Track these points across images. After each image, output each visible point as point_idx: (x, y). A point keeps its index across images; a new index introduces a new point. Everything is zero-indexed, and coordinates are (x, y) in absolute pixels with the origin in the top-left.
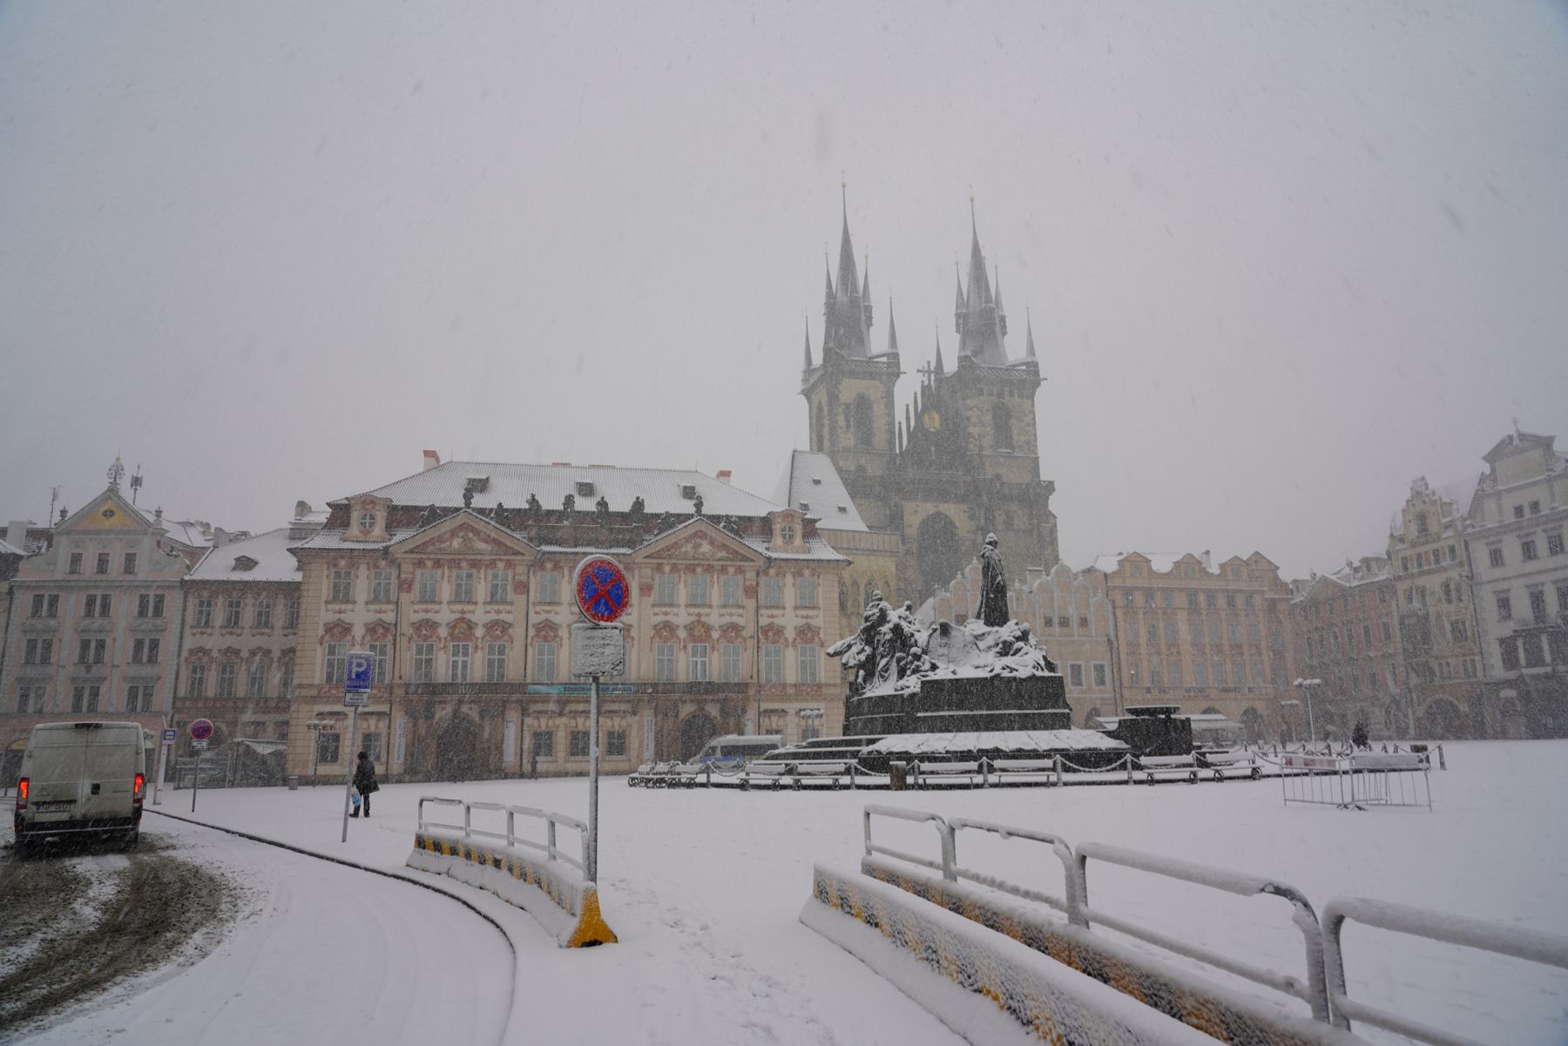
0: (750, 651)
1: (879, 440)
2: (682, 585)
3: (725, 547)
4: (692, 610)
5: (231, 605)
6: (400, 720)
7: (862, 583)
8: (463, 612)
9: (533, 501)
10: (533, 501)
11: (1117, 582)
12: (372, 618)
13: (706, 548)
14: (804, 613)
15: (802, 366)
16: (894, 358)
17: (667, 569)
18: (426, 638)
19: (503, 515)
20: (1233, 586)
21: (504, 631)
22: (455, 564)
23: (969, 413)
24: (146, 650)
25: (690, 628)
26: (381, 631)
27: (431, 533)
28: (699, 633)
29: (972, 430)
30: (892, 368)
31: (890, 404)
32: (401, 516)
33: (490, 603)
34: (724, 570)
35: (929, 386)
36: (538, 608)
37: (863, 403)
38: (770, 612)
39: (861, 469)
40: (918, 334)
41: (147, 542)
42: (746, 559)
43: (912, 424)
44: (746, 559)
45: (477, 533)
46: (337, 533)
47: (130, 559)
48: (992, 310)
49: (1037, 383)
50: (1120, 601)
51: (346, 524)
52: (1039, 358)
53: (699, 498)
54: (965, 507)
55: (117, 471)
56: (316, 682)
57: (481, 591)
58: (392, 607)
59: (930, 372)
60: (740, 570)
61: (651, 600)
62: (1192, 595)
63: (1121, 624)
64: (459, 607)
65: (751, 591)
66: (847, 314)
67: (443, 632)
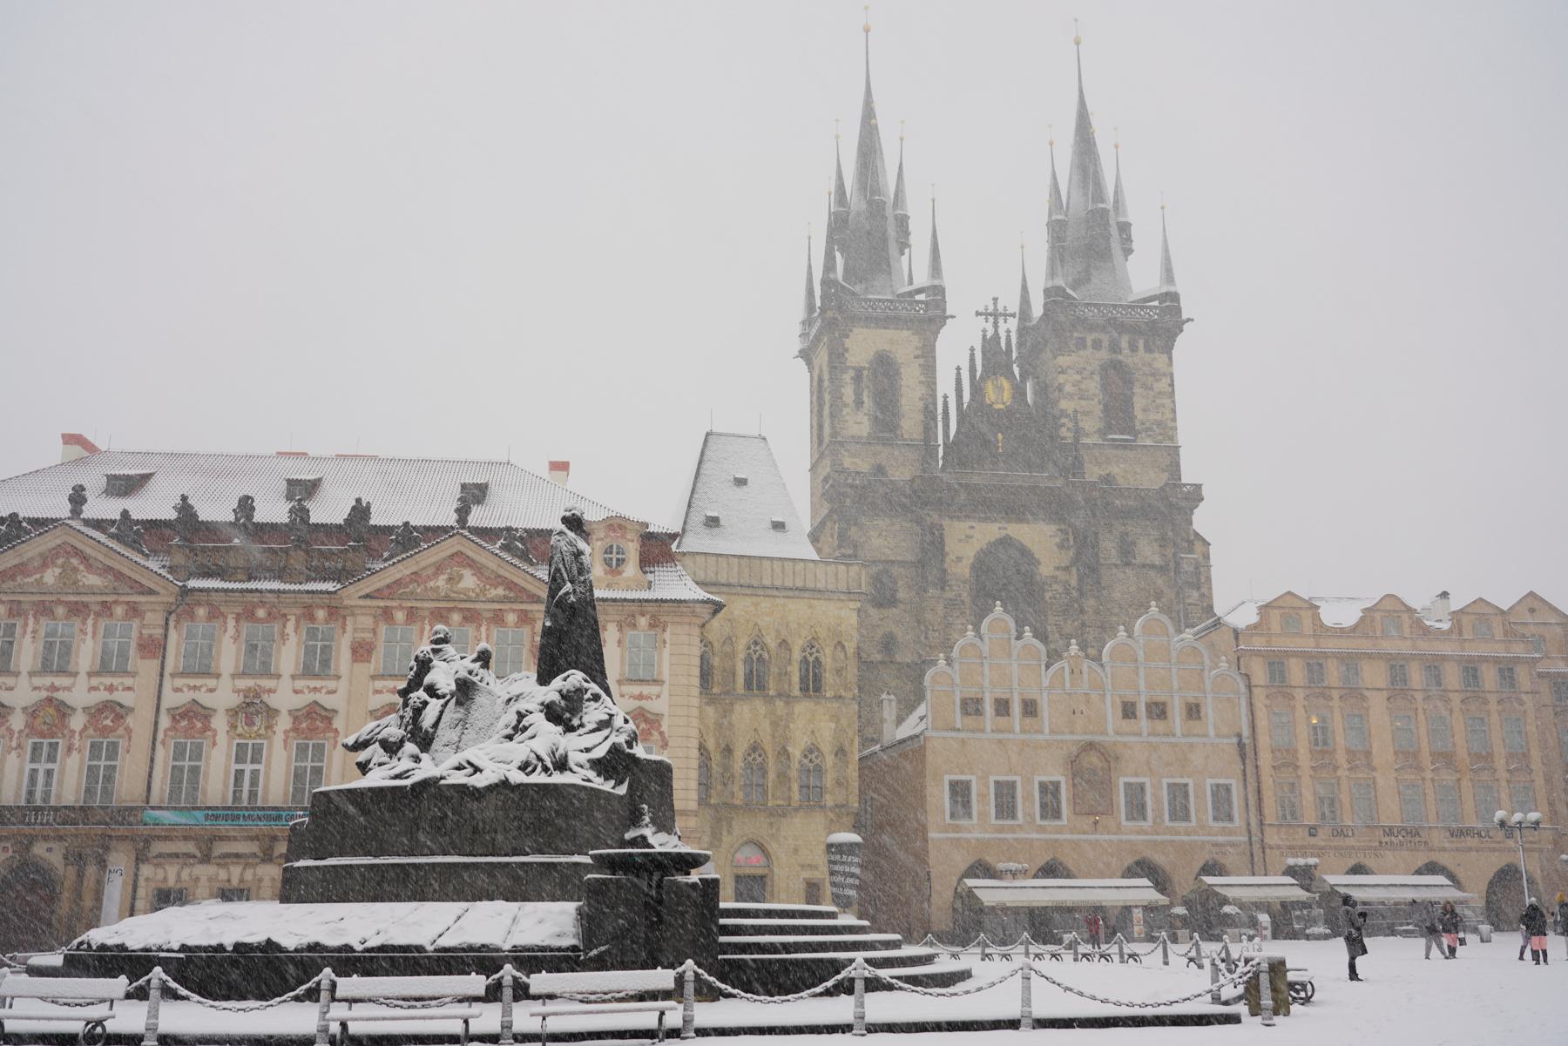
1: (910, 425)
8: (53, 688)
9: (185, 507)
10: (185, 507)
11: (1258, 643)
13: (469, 581)
15: (800, 313)
17: (400, 616)
19: (132, 532)
20: (1474, 651)
21: (119, 718)
22: (44, 610)
31: (929, 368)
35: (996, 335)
36: (179, 682)
37: (885, 366)
39: (880, 470)
43: (966, 397)
45: (85, 559)
48: (1105, 212)
49: (1179, 327)
50: (1260, 674)
52: (1179, 287)
57: (86, 654)
61: (371, 668)
62: (1397, 667)
64: (48, 680)
66: (866, 231)
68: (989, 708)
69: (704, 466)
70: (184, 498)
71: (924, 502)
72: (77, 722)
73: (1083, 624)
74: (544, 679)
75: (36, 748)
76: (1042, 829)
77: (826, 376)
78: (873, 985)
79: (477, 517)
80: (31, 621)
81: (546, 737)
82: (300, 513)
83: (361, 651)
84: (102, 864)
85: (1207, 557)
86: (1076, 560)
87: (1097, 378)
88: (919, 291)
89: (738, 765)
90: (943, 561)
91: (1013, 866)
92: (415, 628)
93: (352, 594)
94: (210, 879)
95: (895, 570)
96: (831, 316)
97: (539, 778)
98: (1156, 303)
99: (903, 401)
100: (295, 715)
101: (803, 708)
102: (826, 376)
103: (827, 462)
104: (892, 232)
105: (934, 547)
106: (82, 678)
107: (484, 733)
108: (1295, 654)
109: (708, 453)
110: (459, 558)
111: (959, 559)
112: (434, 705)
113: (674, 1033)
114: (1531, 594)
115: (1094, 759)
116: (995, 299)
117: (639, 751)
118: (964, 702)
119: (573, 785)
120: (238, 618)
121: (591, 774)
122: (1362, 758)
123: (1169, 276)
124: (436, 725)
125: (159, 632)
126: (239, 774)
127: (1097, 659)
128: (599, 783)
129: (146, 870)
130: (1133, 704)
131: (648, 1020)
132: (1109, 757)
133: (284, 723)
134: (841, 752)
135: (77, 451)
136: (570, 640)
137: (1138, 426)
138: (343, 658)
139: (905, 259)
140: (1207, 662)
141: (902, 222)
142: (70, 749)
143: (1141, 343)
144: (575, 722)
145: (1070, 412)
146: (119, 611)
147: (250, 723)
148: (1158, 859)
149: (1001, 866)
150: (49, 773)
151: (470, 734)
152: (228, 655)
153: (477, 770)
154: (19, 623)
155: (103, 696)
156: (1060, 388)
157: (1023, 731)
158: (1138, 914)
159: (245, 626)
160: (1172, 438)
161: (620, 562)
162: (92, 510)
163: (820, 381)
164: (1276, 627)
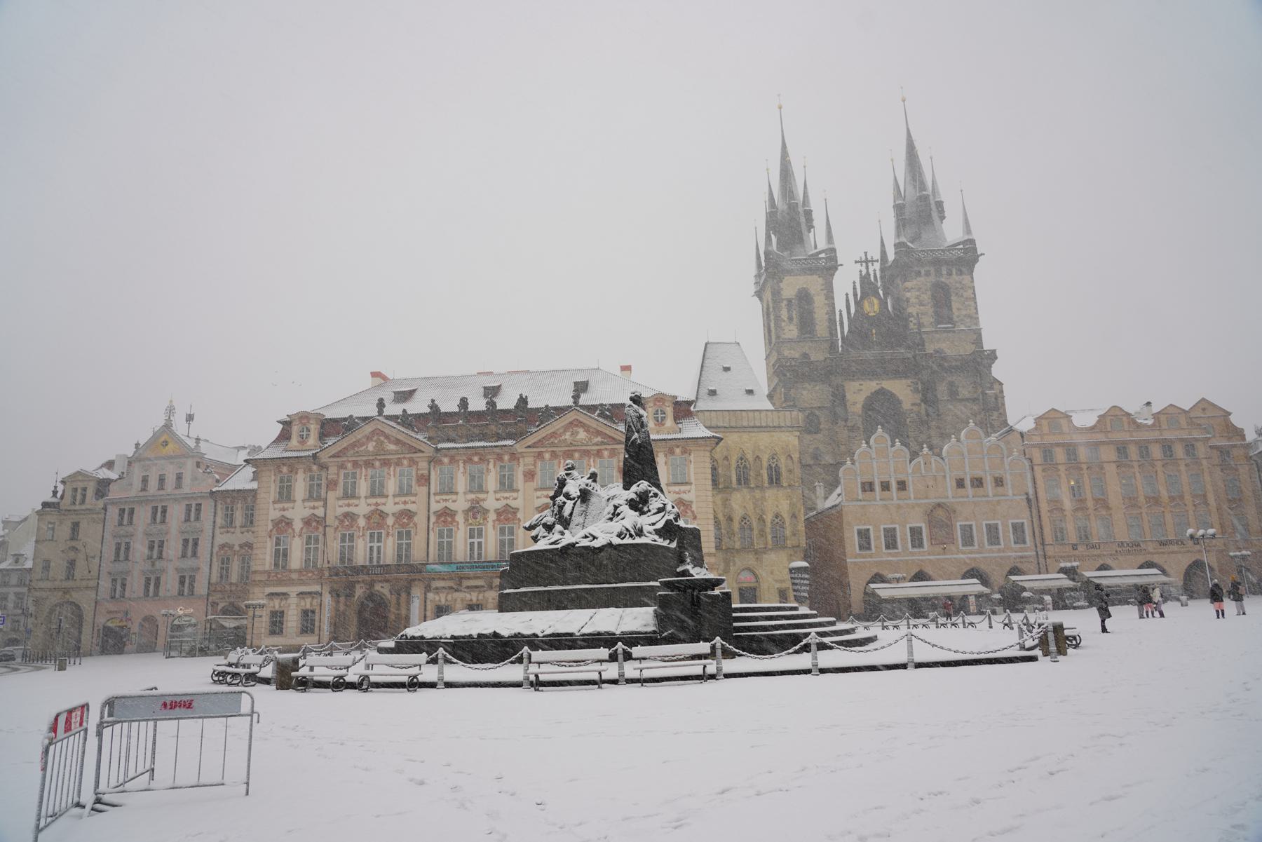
1: (821, 329)
3: (598, 433)
5: (247, 509)
6: (327, 599)
8: (377, 504)
9: (434, 406)
10: (434, 406)
11: (1037, 440)
12: (307, 513)
13: (582, 435)
14: (677, 488)
15: (753, 270)
17: (547, 456)
19: (406, 420)
20: (1169, 435)
22: (368, 464)
23: (908, 295)
24: (190, 546)
26: (314, 524)
27: (351, 439)
32: (330, 427)
33: (399, 495)
34: (599, 453)
36: (438, 498)
37: (804, 297)
39: (805, 355)
41: (190, 464)
43: (853, 310)
45: (387, 437)
46: (283, 446)
47: (179, 477)
49: (975, 260)
50: (1037, 456)
51: (289, 438)
52: (975, 236)
54: (909, 381)
55: (171, 410)
56: (267, 567)
57: (391, 486)
58: (321, 503)
59: (867, 261)
62: (1122, 449)
63: (1040, 483)
64: (373, 501)
66: (788, 221)
67: (362, 522)
68: (877, 487)
69: (706, 362)
71: (833, 372)
72: (390, 521)
74: (627, 487)
75: (372, 536)
76: (912, 554)
78: (822, 647)
79: (585, 399)
81: (630, 518)
82: (492, 404)
83: (529, 475)
84: (409, 594)
86: (925, 400)
88: (820, 253)
89: (736, 526)
91: (897, 575)
92: (556, 462)
94: (462, 600)
95: (817, 413)
96: (771, 271)
97: (628, 541)
101: (771, 494)
103: (775, 353)
104: (803, 220)
105: (839, 397)
106: (391, 498)
107: (596, 519)
108: (1058, 445)
109: (708, 355)
111: (854, 403)
112: (569, 504)
113: (713, 677)
115: (940, 513)
117: (681, 523)
118: (863, 484)
119: (647, 544)
120: (465, 462)
121: (656, 537)
122: (1103, 503)
123: (968, 230)
124: (571, 514)
125: (426, 472)
126: (472, 544)
127: (939, 455)
128: (661, 542)
129: (430, 596)
130: (962, 480)
131: (698, 670)
132: (950, 511)
133: (492, 516)
134: (794, 516)
135: (378, 381)
136: (639, 463)
137: (955, 319)
138: (519, 481)
139: (811, 235)
140: (1005, 452)
141: (808, 214)
143: (954, 271)
144: (645, 509)
146: (405, 462)
148: (983, 567)
149: (890, 576)
151: (590, 518)
152: (461, 483)
153: (595, 538)
154: (358, 471)
155: (402, 507)
156: (908, 300)
157: (899, 499)
158: (972, 599)
159: (468, 467)
160: (977, 323)
161: (663, 419)
162: (387, 411)
163: (768, 309)
164: (1046, 429)
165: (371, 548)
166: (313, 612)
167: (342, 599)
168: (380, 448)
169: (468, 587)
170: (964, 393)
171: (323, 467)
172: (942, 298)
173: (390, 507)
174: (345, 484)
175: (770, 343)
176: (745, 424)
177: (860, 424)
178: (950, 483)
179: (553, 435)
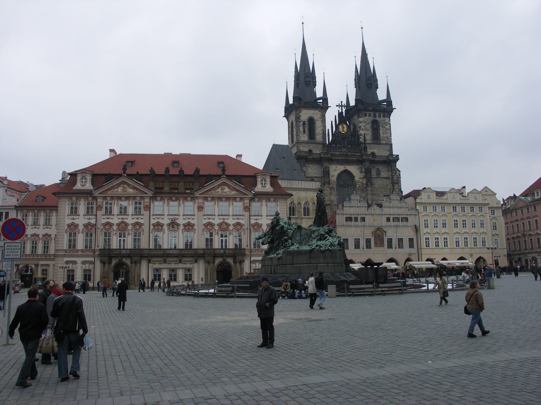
0: (246, 234)
1: (319, 138)
2: (216, 206)
3: (235, 189)
4: (220, 217)
6: (98, 264)
7: (303, 203)
8: (123, 219)
9: (152, 170)
10: (152, 170)
12: (86, 221)
13: (227, 189)
16: (325, 99)
18: (108, 230)
23: (360, 125)
25: (220, 225)
26: (90, 227)
28: (224, 227)
29: (362, 132)
30: (324, 106)
36: (154, 217)
37: (311, 121)
38: (255, 218)
39: (310, 151)
40: (337, 87)
42: (245, 194)
44: (245, 194)
53: (224, 167)
59: (342, 106)
60: (242, 199)
61: (203, 213)
64: (121, 217)
65: (247, 209)
67: (115, 227)
70: (152, 168)
72: (130, 227)
73: (367, 194)
77: (294, 123)
80: (116, 201)
83: (201, 208)
84: (140, 264)
85: (400, 175)
87: (370, 124)
90: (329, 177)
93: (197, 194)
98: (385, 103)
99: (317, 131)
100: (184, 225)
102: (294, 123)
105: (326, 173)
110: (224, 184)
111: (333, 176)
114: (486, 187)
115: (379, 232)
116: (342, 102)
129: (150, 265)
133: (181, 227)
142: (129, 234)
145: (363, 134)
147: (173, 227)
148: (395, 257)
150: (124, 240)
153: (320, 247)
155: (136, 221)
156: (360, 127)
160: (391, 141)
165: (120, 240)
166: (90, 270)
167: (107, 265)
168: (124, 190)
169: (154, 261)
170: (384, 174)
171: (95, 198)
172: (375, 127)
173: (130, 221)
174: (106, 208)
175: (292, 142)
176: (295, 187)
177: (335, 186)
178: (384, 219)
179: (213, 189)
